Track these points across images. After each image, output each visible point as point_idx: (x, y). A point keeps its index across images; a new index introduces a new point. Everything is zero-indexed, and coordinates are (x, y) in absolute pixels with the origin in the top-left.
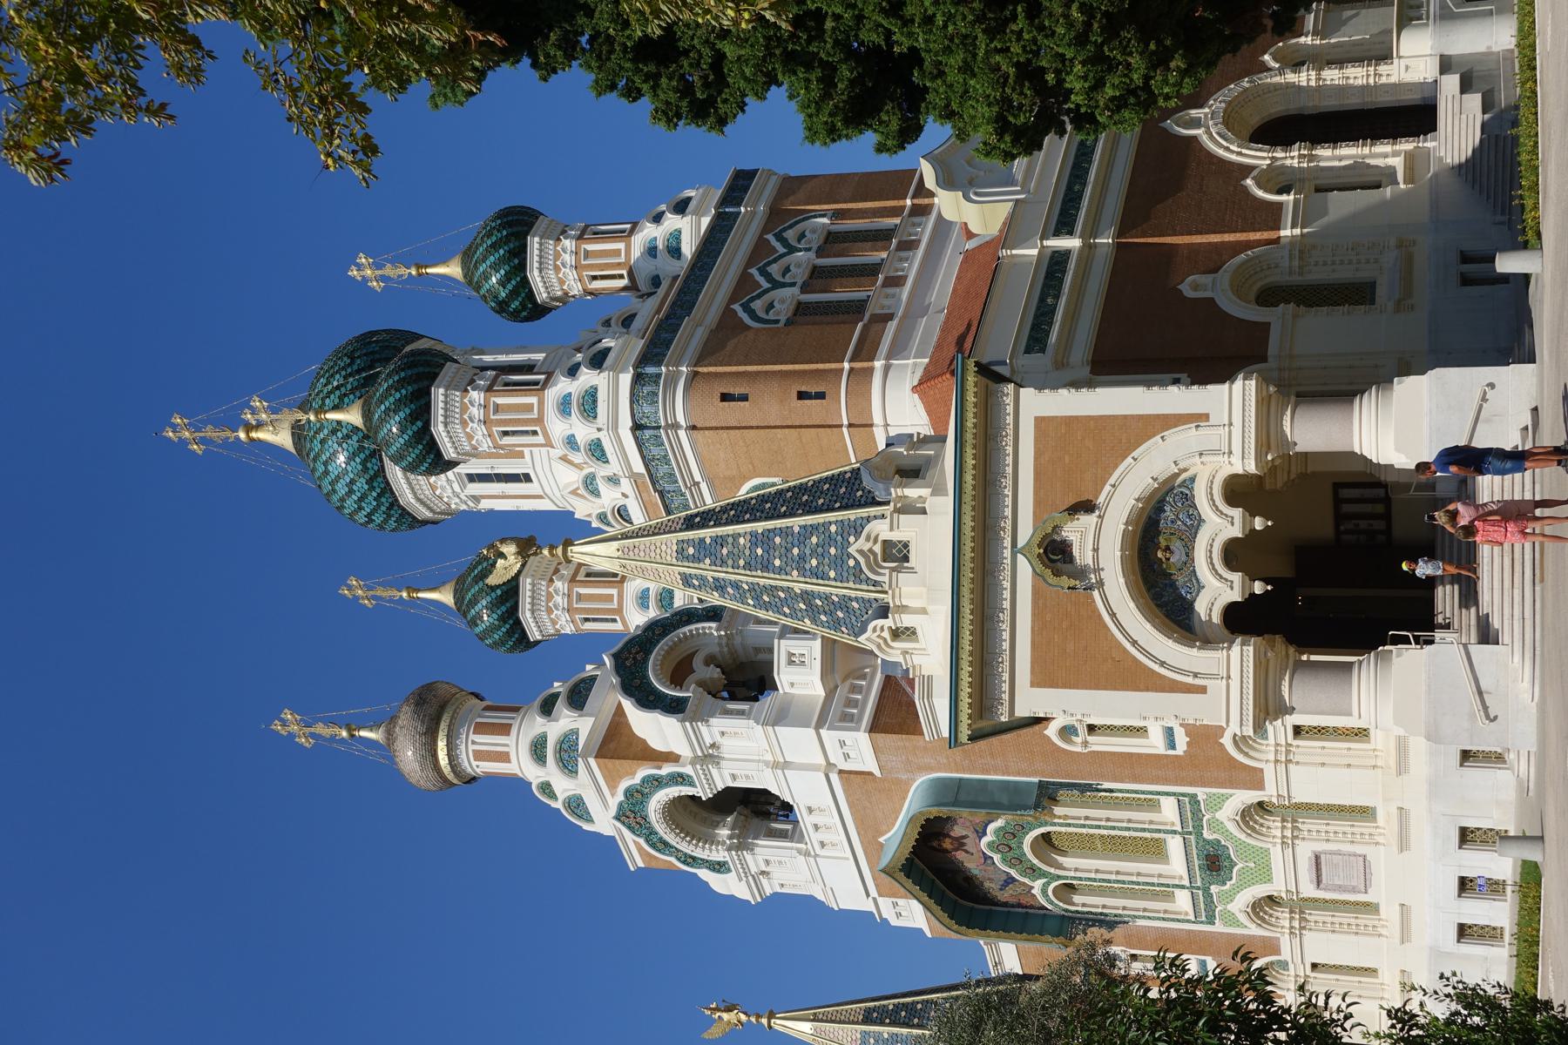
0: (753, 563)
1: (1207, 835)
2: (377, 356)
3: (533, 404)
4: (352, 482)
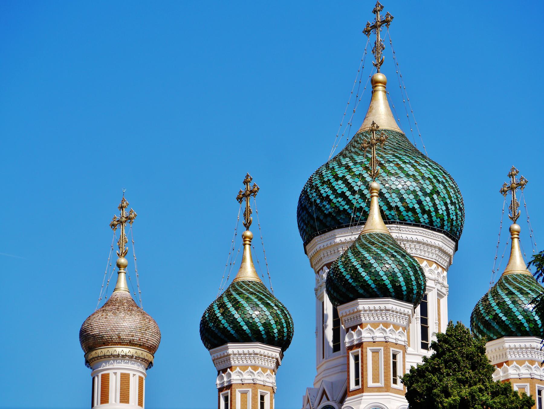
2: (433, 214)
4: (330, 201)
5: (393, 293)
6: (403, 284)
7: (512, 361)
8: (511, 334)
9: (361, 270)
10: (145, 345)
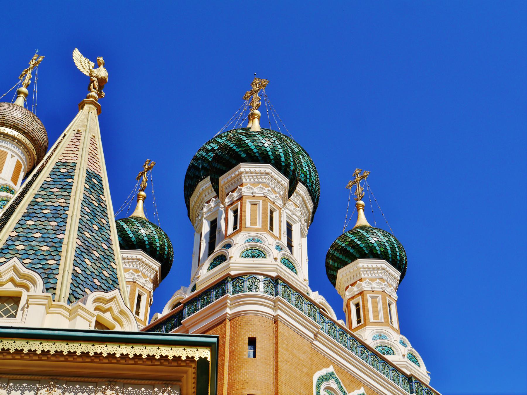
0: (36, 207)
3: (257, 225)
5: (273, 161)
6: (282, 155)
7: (366, 278)
8: (364, 256)
9: (244, 139)
10: (29, 134)
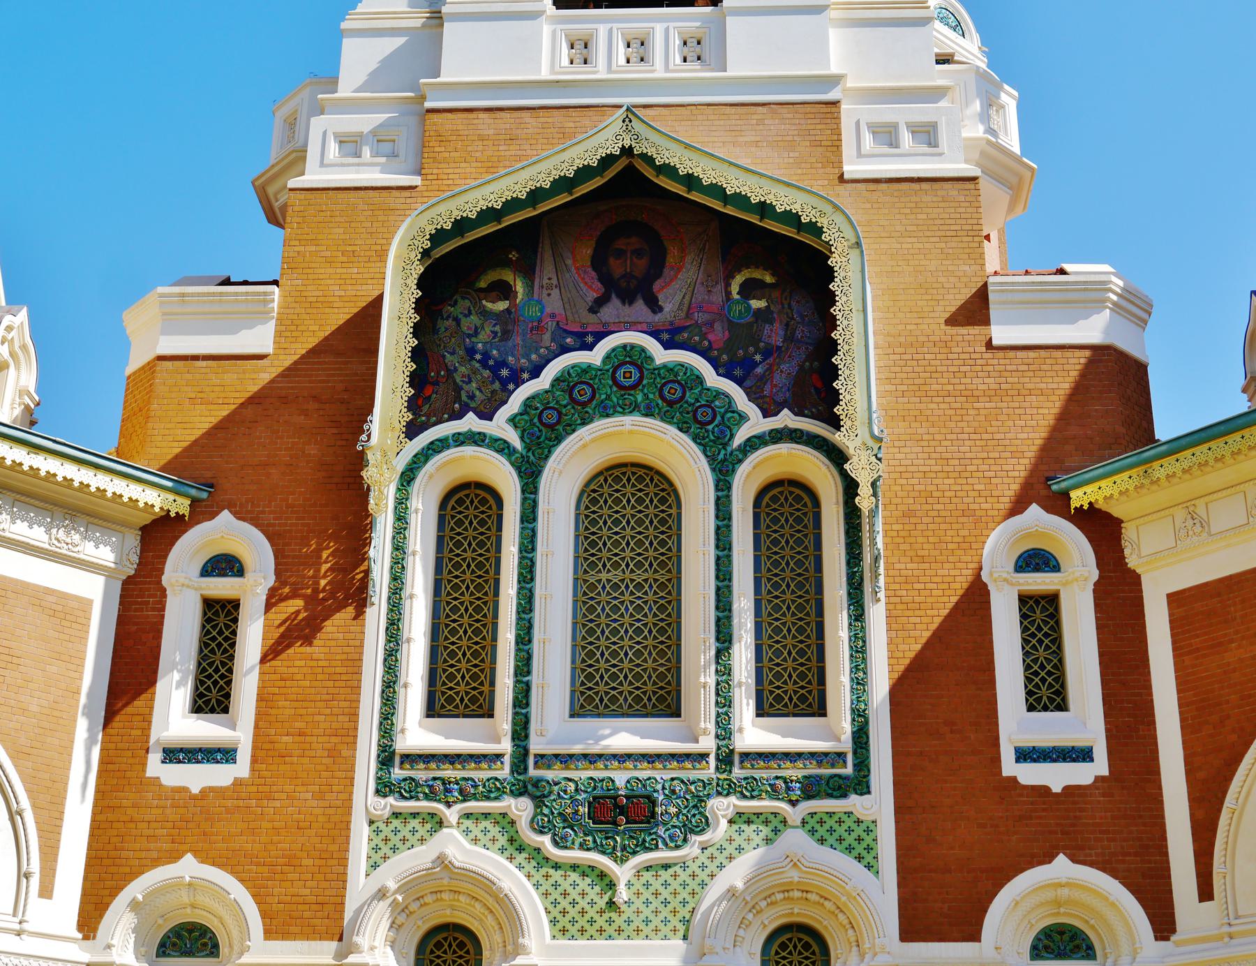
1: (721, 807)
